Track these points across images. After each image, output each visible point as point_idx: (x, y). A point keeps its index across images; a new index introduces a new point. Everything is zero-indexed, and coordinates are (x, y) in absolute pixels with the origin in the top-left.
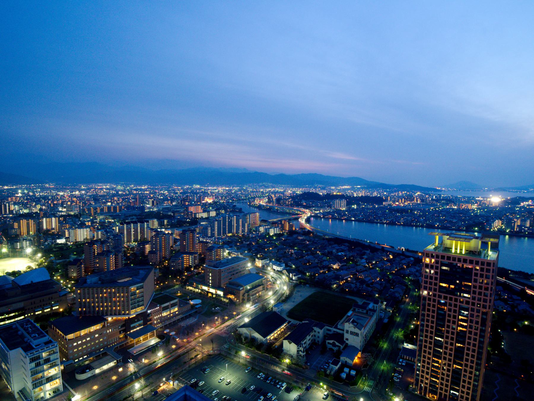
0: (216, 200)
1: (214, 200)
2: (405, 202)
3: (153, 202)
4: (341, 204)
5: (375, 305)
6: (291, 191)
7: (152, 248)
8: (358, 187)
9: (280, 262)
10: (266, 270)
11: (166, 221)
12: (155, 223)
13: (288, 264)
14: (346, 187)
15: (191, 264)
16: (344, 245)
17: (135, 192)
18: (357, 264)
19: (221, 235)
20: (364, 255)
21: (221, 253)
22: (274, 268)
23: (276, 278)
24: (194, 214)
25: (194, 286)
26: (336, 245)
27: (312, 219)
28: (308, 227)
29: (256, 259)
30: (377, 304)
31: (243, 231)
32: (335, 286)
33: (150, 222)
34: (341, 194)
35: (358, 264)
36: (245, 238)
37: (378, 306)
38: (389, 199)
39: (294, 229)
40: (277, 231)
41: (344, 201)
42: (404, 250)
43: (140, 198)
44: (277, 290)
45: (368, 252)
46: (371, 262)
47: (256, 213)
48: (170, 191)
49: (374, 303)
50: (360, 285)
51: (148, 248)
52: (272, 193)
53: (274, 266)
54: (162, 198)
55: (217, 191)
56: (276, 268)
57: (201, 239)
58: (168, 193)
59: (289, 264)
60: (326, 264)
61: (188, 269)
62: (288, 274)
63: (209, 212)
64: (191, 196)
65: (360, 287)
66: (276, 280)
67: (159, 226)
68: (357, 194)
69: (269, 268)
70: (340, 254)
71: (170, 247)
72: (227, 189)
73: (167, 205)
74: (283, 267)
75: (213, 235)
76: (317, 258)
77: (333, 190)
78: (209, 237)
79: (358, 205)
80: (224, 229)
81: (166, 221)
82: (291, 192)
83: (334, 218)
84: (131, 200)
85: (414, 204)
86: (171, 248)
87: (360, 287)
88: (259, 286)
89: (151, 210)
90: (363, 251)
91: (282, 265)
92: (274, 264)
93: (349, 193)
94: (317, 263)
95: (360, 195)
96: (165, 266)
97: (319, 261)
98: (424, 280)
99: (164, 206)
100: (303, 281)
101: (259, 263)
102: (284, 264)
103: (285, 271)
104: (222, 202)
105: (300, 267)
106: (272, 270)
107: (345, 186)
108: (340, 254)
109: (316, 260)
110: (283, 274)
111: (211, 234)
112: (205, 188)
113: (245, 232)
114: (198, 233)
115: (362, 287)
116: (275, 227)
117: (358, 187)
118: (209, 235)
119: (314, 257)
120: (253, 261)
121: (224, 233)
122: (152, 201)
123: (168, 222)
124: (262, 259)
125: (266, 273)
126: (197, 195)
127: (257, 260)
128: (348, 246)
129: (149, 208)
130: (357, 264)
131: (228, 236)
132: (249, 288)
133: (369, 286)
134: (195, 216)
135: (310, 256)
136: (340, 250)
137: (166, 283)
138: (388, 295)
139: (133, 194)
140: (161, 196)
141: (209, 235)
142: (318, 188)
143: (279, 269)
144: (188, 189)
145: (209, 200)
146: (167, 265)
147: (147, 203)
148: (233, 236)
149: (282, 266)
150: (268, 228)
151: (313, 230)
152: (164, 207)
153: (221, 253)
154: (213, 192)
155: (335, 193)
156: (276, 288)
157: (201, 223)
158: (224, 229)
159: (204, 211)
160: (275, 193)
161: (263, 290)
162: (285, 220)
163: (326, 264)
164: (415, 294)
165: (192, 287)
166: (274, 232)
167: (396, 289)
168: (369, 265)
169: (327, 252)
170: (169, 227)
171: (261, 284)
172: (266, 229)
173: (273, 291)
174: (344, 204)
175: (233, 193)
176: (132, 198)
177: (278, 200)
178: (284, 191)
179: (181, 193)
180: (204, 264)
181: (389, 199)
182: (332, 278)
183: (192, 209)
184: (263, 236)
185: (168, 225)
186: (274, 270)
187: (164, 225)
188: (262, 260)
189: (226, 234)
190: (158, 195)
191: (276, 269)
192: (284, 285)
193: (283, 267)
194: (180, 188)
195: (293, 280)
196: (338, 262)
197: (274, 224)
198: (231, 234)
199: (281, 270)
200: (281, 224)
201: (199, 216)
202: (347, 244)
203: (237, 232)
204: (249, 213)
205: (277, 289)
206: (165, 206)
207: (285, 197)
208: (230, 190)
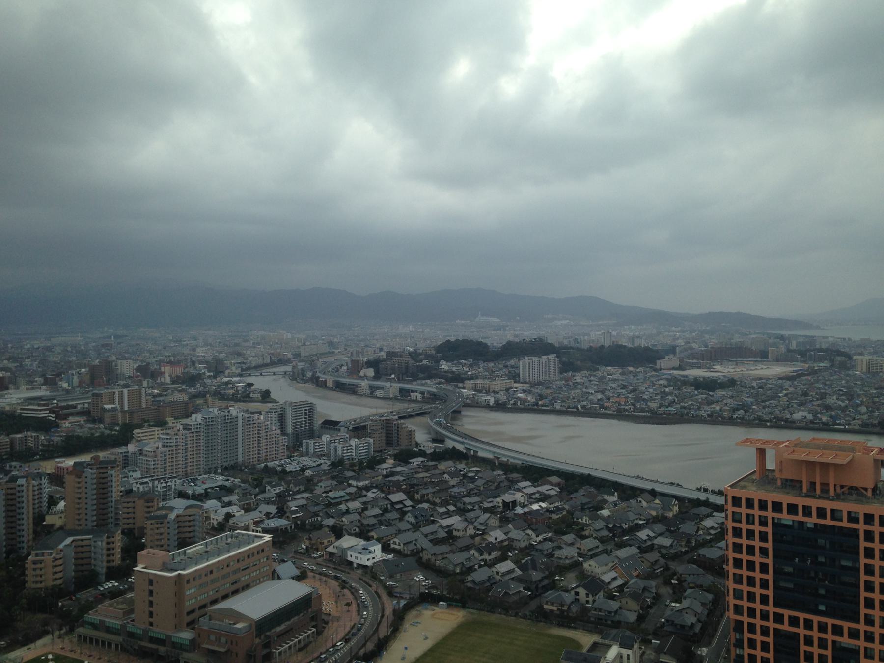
5: (625, 652)
9: (368, 539)
13: (392, 546)
18: (584, 533)
20: (602, 509)
26: (528, 483)
30: (630, 647)
35: (587, 533)
37: (630, 652)
45: (614, 498)
49: (622, 646)
50: (587, 595)
56: (356, 558)
59: (395, 543)
65: (588, 602)
70: (535, 507)
76: (472, 523)
87: (588, 602)
90: (599, 498)
91: (372, 549)
94: (472, 537)
97: (478, 530)
98: (734, 574)
102: (379, 546)
105: (424, 552)
108: (535, 507)
109: (471, 527)
115: (594, 601)
119: (466, 520)
128: (558, 485)
130: (584, 533)
133: (613, 598)
135: (454, 518)
136: (537, 495)
138: (663, 620)
163: (496, 539)
167: (686, 603)
169: (501, 505)
182: (512, 579)
202: (555, 479)
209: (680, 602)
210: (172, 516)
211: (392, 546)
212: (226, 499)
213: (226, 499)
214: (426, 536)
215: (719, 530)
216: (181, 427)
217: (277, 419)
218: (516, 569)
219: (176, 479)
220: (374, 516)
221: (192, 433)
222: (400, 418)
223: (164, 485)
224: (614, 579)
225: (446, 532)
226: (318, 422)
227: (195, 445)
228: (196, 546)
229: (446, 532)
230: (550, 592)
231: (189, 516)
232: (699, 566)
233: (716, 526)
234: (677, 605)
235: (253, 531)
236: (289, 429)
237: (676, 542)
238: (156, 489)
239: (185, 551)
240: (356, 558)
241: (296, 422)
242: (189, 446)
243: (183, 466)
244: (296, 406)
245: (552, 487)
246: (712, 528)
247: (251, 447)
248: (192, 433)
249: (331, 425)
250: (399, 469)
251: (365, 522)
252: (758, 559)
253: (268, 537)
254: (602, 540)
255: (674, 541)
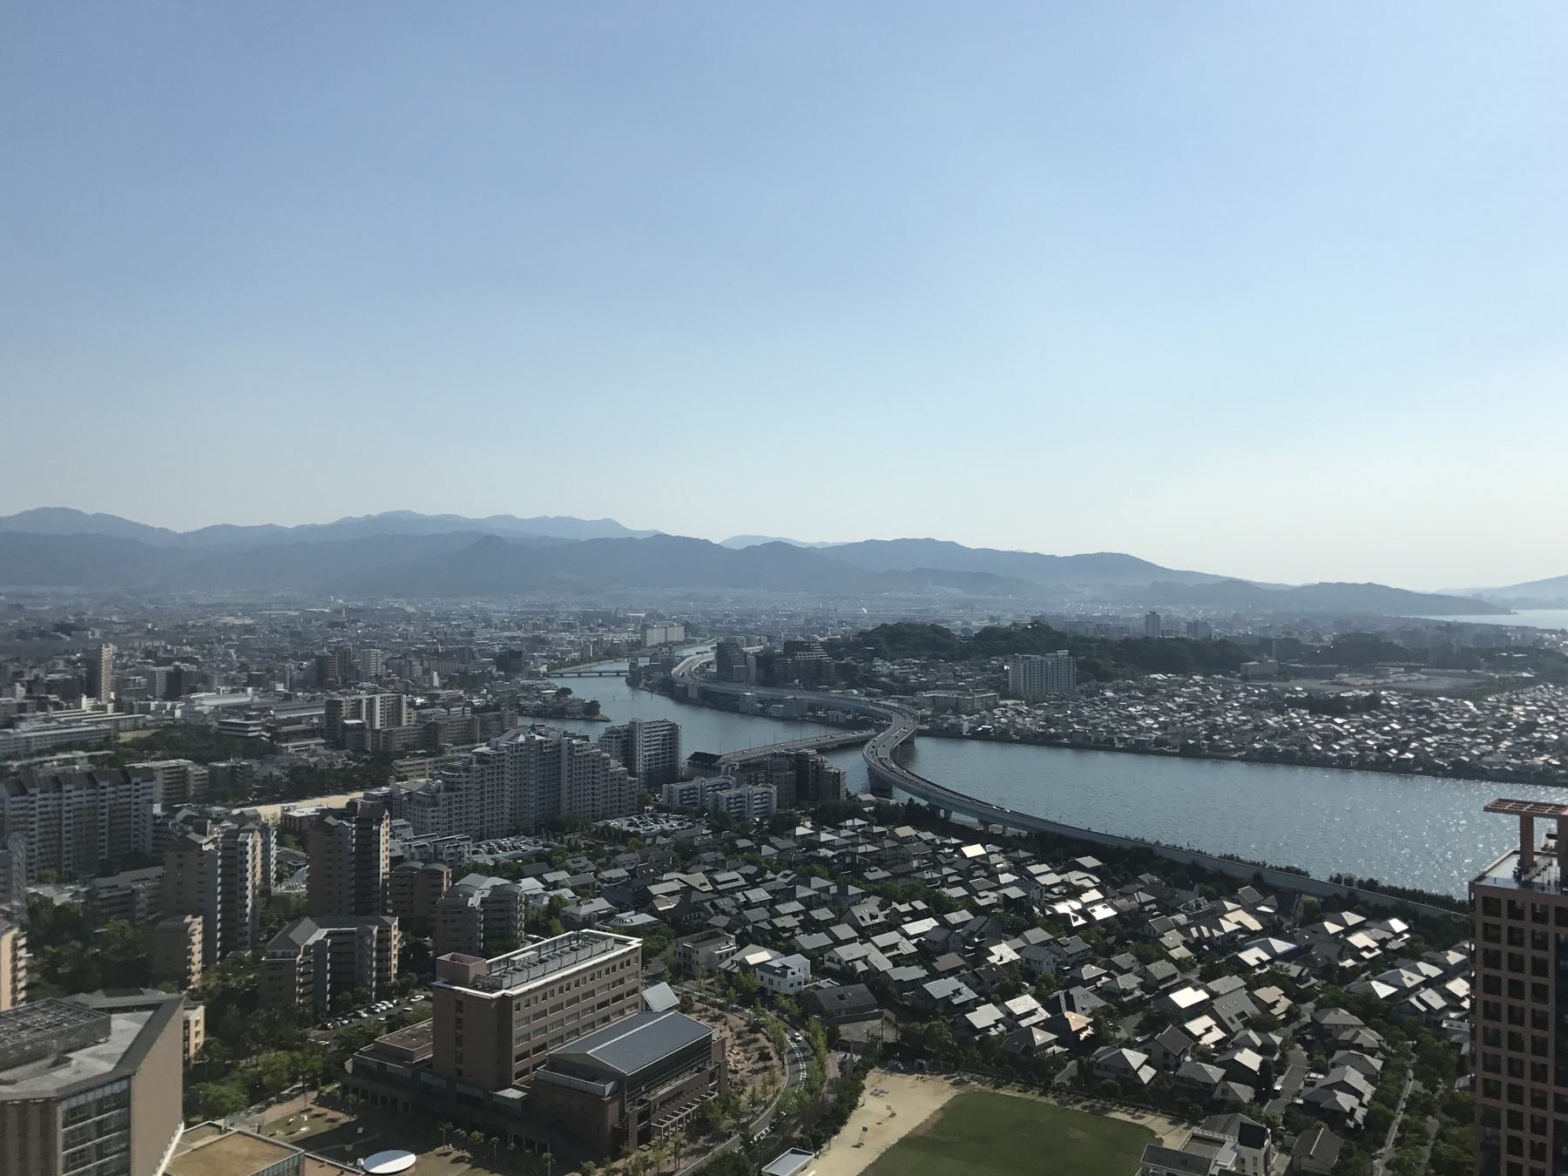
5: (1247, 1151)
16: (1082, 868)
26: (1045, 868)
60: (1001, 959)
128: (1093, 871)
163: (1001, 959)
182: (1035, 1025)
202: (1089, 861)
209: (1325, 1072)
210: (474, 901)
211: (828, 964)
212: (550, 877)
213: (550, 877)
214: (883, 950)
215: (1378, 952)
216: (475, 757)
217: (619, 749)
218: (1041, 1010)
219: (470, 842)
220: (795, 914)
221: (493, 768)
222: (821, 751)
223: (452, 850)
224: (1208, 1030)
225: (914, 945)
226: (685, 752)
227: (496, 788)
228: (524, 952)
229: (914, 945)
230: (1102, 1049)
231: (502, 902)
232: (1352, 1013)
233: (1373, 944)
234: (1320, 1076)
235: (598, 929)
236: (640, 767)
237: (1307, 970)
238: (440, 857)
239: (508, 957)
240: (771, 982)
241: (649, 755)
242: (486, 789)
243: (477, 822)
244: (653, 726)
245: (1086, 875)
246: (1367, 949)
247: (582, 793)
248: (493, 768)
249: (704, 762)
250: (824, 837)
251: (778, 922)
252: (1527, 1004)
253: (635, 942)
254: (1179, 964)
255: (1303, 970)
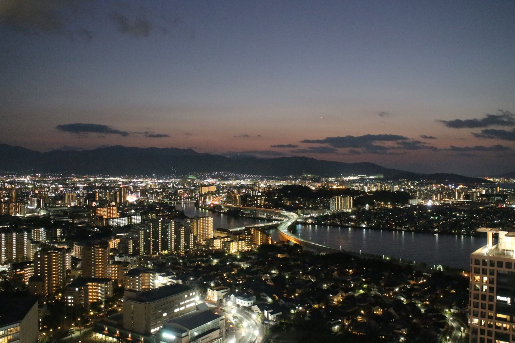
0: (142, 199)
1: (139, 199)
2: (441, 199)
3: (39, 202)
4: (344, 203)
6: (264, 184)
7: (36, 272)
8: (370, 177)
10: (226, 306)
11: (59, 232)
12: (42, 234)
14: (352, 178)
15: (100, 298)
17: (9, 186)
19: (150, 254)
21: (151, 281)
22: (237, 303)
23: (241, 318)
24: (106, 219)
25: (106, 332)
27: (299, 227)
28: (293, 240)
29: (208, 289)
31: (187, 247)
32: (336, 327)
33: (34, 231)
34: (344, 187)
36: (190, 257)
38: (418, 195)
39: (270, 243)
40: (242, 246)
41: (350, 199)
42: (442, 270)
43: (17, 196)
44: (243, 337)
46: (393, 290)
47: (208, 217)
48: (68, 184)
51: (28, 273)
52: (235, 188)
53: (238, 300)
54: (53, 195)
55: (143, 184)
56: (242, 303)
57: (117, 259)
58: (63, 187)
61: (95, 306)
62: (260, 312)
63: (129, 216)
64: (102, 193)
66: (241, 321)
67: (47, 240)
68: (369, 188)
69: (230, 303)
71: (65, 271)
72: (161, 181)
73: (61, 207)
74: (252, 301)
75: (136, 252)
77: (331, 182)
78: (130, 256)
79: (372, 204)
80: (156, 245)
81: (59, 232)
82: (265, 186)
83: (334, 226)
84: (2, 198)
85: (455, 202)
86: (67, 273)
88: (213, 330)
89: (36, 214)
92: (237, 295)
93: (356, 187)
95: (374, 190)
96: (57, 301)
99: (56, 207)
100: (286, 321)
101: (213, 295)
102: (255, 297)
103: (256, 308)
104: (152, 201)
106: (234, 307)
107: (351, 176)
110: (253, 311)
111: (133, 250)
112: (124, 180)
113: (189, 248)
114: (112, 249)
116: (240, 240)
117: (370, 177)
118: (131, 251)
120: (204, 293)
121: (156, 249)
122: (38, 199)
123: (61, 233)
124: (217, 287)
125: (224, 311)
126: (110, 191)
127: (209, 291)
129: (32, 211)
131: (162, 255)
132: (196, 334)
134: (107, 223)
137: (59, 328)
139: (6, 190)
140: (52, 192)
141: (131, 251)
142: (309, 180)
143: (245, 303)
144: (95, 182)
145: (131, 199)
146: (61, 299)
147: (29, 202)
148: (172, 254)
149: (252, 300)
150: (228, 241)
151: (300, 243)
152: (57, 209)
153: (151, 281)
154: (137, 187)
155: (335, 187)
156: (241, 335)
157: (117, 235)
158: (156, 245)
159: (122, 216)
160: (239, 188)
161: (220, 337)
162: (257, 228)
164: (460, 334)
165: (103, 334)
166: (238, 248)
168: (389, 294)
170: (64, 240)
171: (216, 327)
172: (224, 243)
173: (236, 337)
174: (350, 203)
175: (170, 188)
176: (4, 196)
177: (244, 198)
178: (253, 185)
179: (84, 188)
180: (121, 298)
181: (418, 195)
183: (102, 212)
184: (219, 254)
185: (62, 238)
186: (238, 306)
187: (56, 237)
188: (217, 290)
189: (158, 251)
190: (48, 192)
191: (241, 305)
192: (254, 328)
193: (252, 301)
194: (83, 180)
195: (269, 321)
196: (342, 291)
197: (237, 236)
198: (166, 252)
199: (250, 305)
200: (250, 234)
201: (113, 223)
203: (177, 248)
204: (198, 218)
205: (243, 335)
206: (58, 207)
207: (255, 193)
208: (164, 183)
